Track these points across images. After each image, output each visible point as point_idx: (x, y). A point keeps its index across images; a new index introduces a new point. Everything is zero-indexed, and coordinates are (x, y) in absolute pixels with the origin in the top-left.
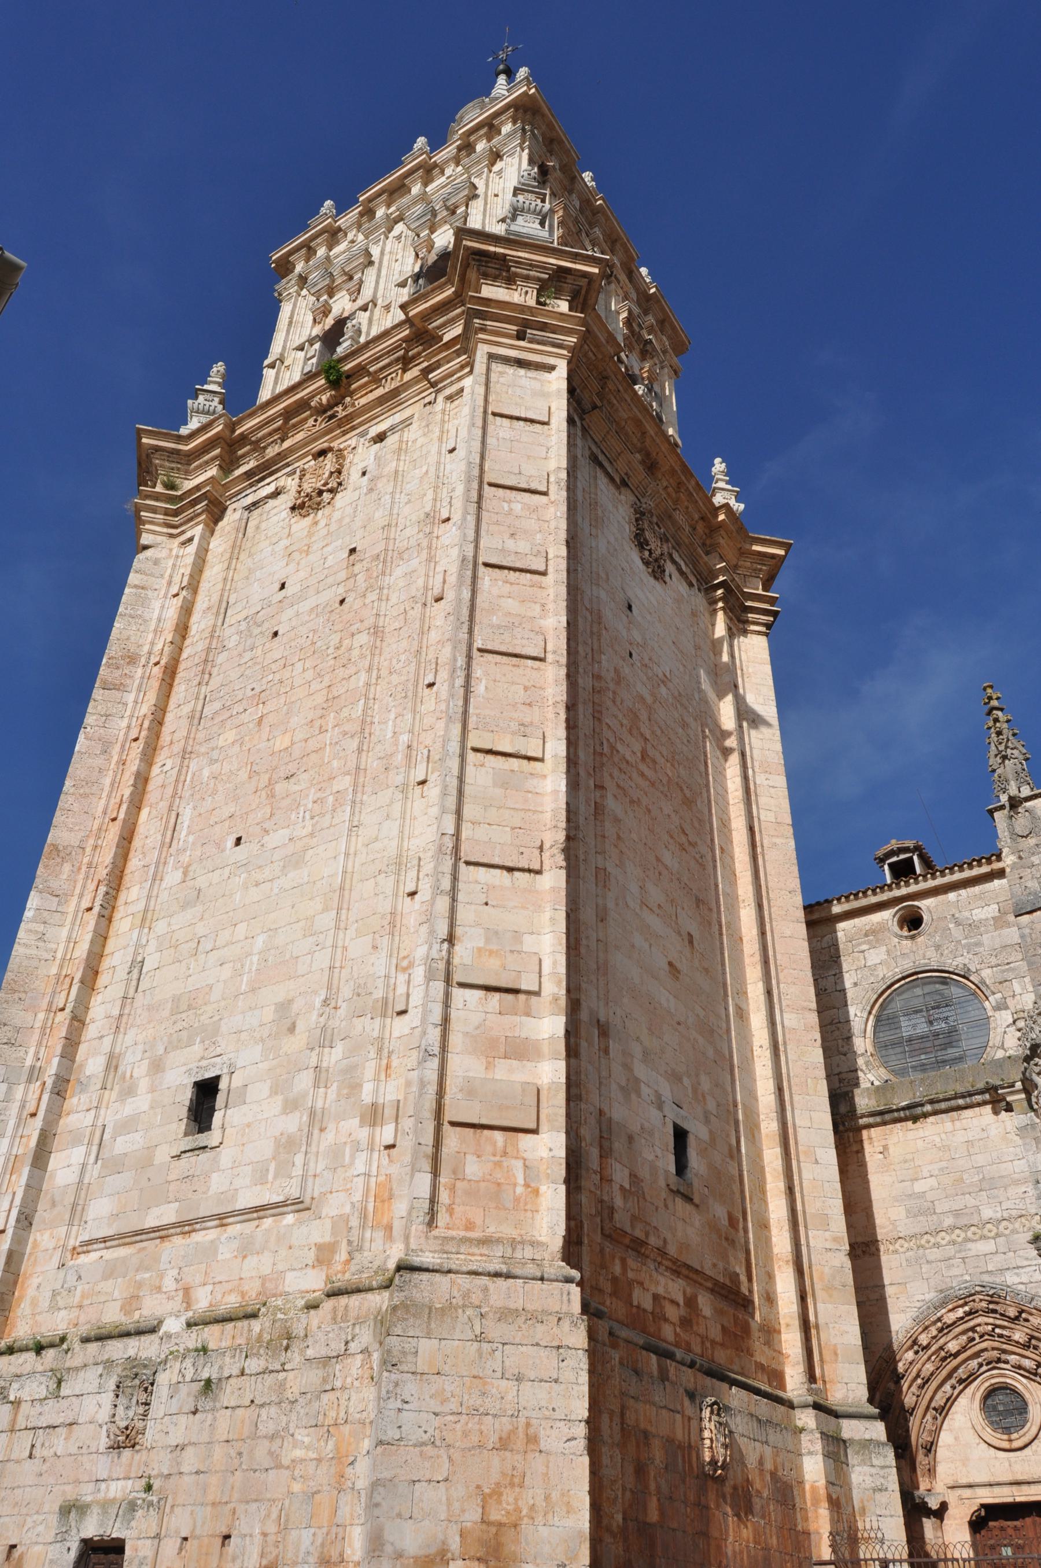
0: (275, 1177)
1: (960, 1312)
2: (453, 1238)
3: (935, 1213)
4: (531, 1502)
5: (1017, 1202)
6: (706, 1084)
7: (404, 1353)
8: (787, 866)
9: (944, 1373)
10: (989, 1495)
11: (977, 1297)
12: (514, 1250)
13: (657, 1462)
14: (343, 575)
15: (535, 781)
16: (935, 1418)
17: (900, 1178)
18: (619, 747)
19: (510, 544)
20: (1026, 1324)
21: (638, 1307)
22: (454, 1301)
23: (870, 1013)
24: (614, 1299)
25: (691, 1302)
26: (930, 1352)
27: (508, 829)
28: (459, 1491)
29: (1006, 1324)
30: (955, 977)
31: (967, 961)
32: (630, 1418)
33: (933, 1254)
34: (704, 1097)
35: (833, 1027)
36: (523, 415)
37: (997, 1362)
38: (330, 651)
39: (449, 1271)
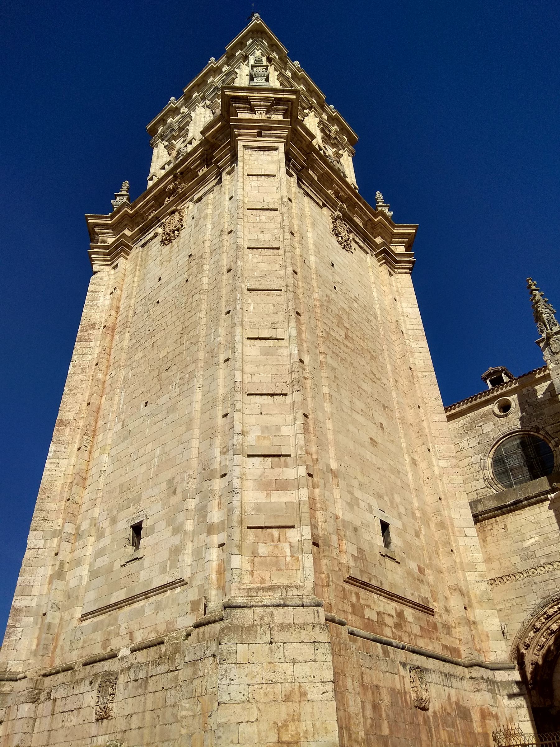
0: (170, 569)
2: (253, 588)
3: (536, 557)
4: (305, 729)
6: (397, 499)
7: (229, 653)
8: (432, 386)
12: (287, 592)
13: (386, 701)
14: (186, 268)
15: (282, 350)
17: (515, 541)
18: (332, 333)
19: (261, 236)
21: (368, 619)
22: (255, 622)
24: (353, 616)
25: (400, 615)
26: (542, 631)
27: (270, 375)
28: (264, 726)
30: (531, 433)
31: (537, 424)
32: (367, 679)
33: (537, 579)
34: (397, 506)
35: (470, 467)
36: (263, 173)
38: (183, 305)
39: (252, 606)
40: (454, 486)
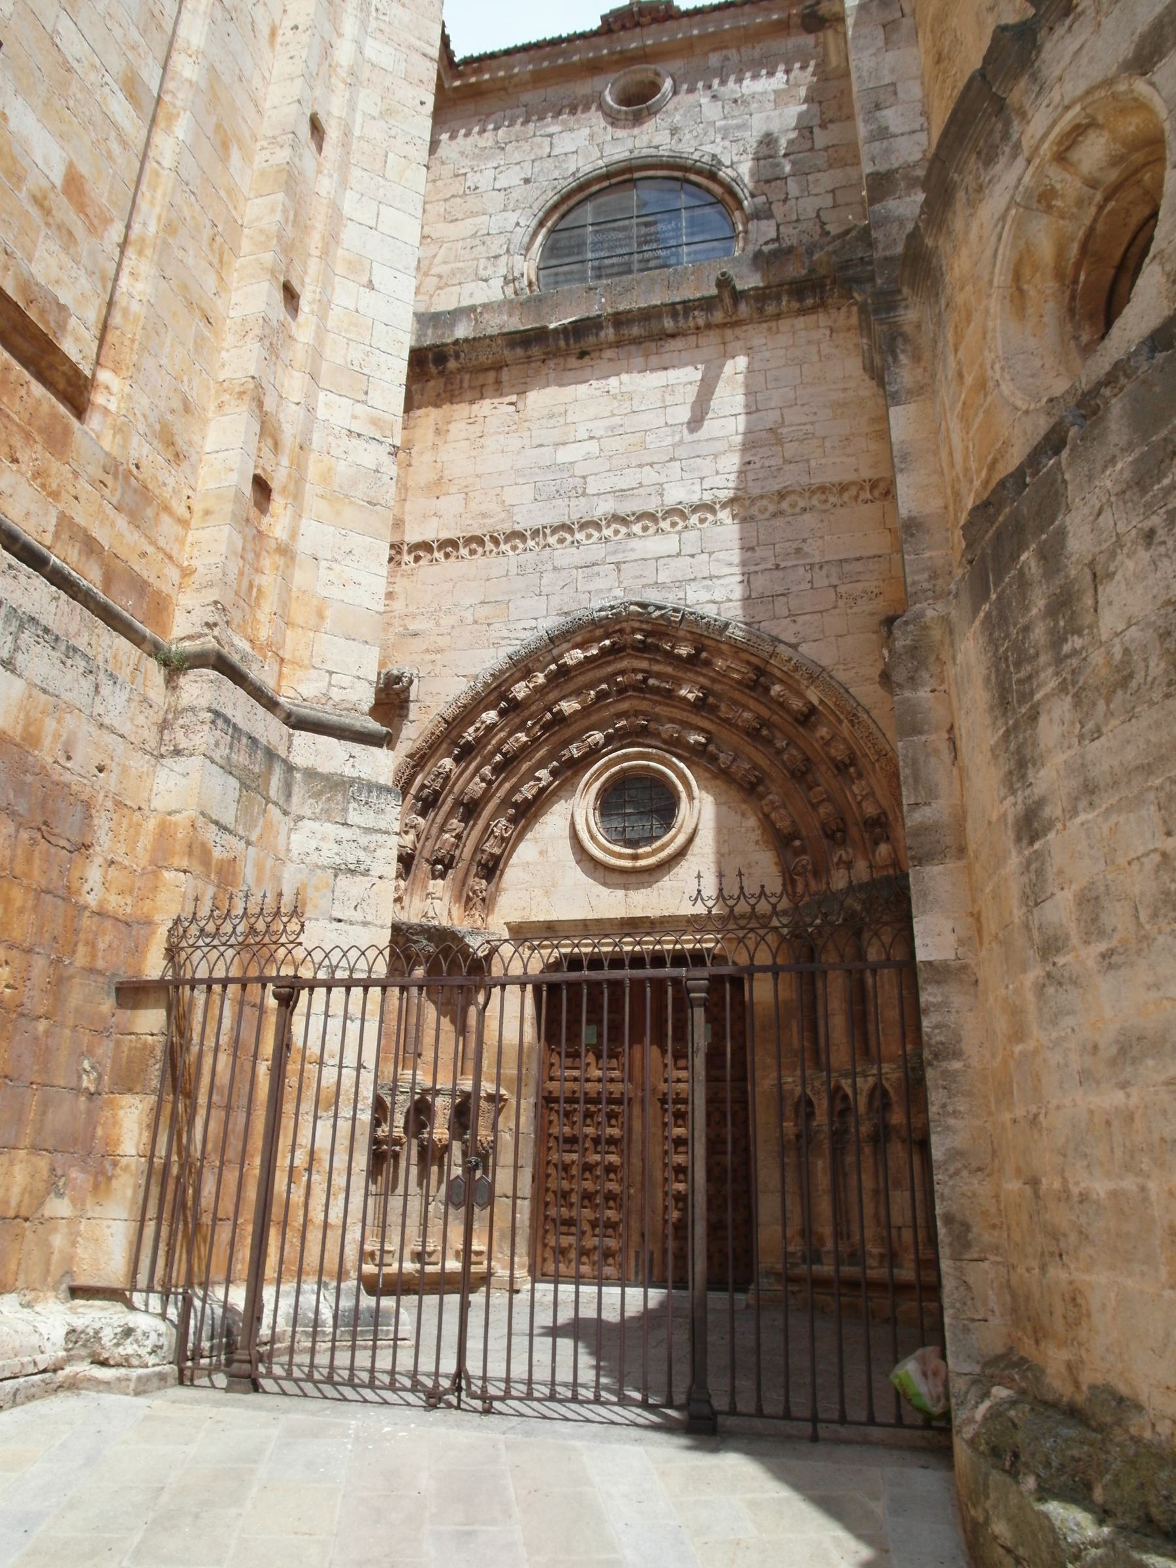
3: (584, 494)
23: (541, 224)
26: (527, 713)
29: (669, 670)
31: (717, 150)
37: (638, 735)
40: (392, 133)
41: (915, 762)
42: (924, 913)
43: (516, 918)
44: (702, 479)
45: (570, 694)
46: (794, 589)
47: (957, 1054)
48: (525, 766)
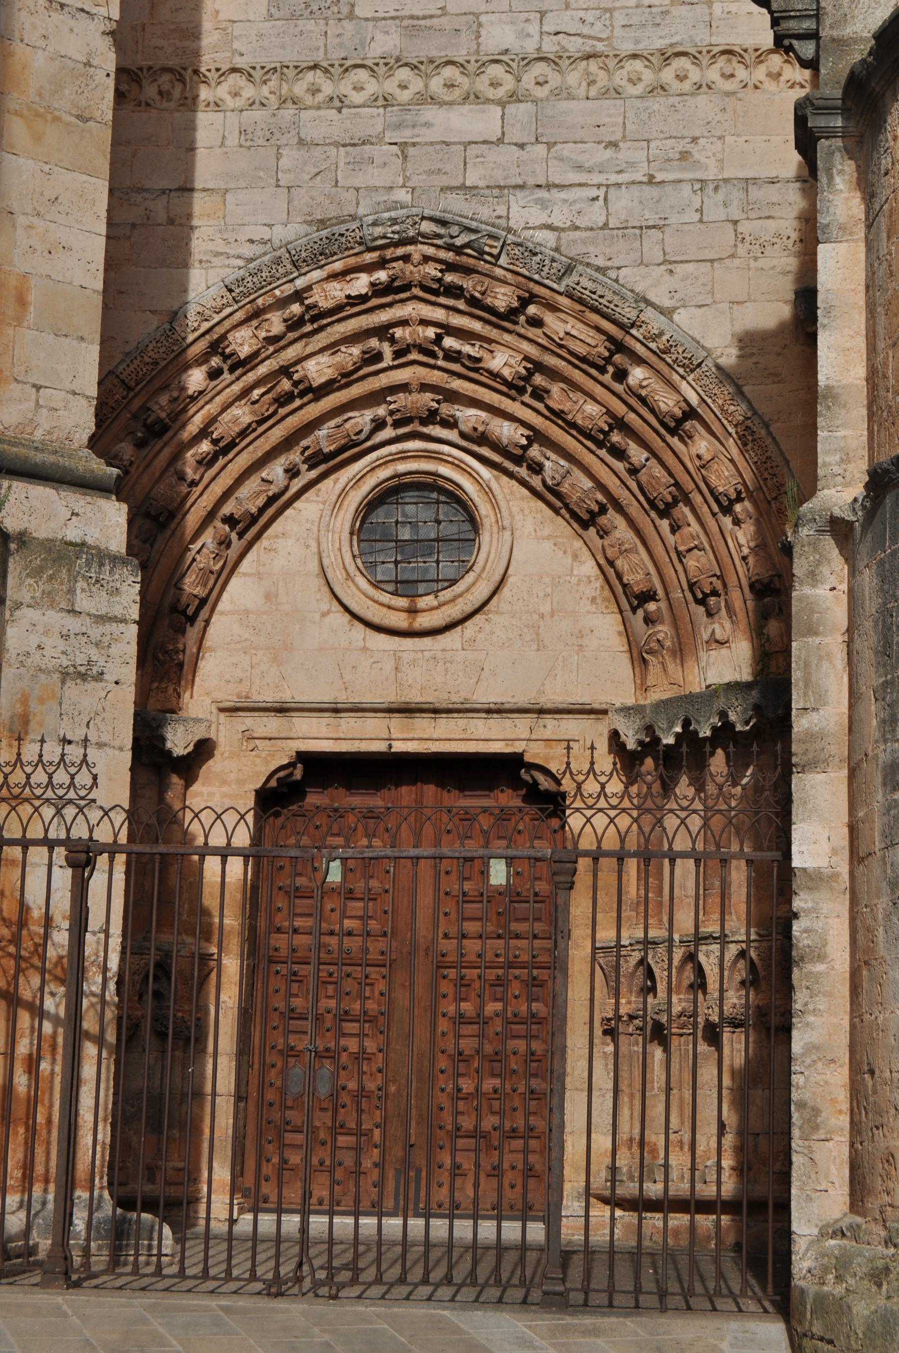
1: (361, 284)
3: (351, 16)
5: (590, 16)
9: (278, 434)
10: (324, 732)
11: (416, 251)
16: (225, 543)
20: (532, 332)
26: (251, 377)
29: (477, 326)
37: (424, 422)
41: (807, 665)
42: (803, 820)
43: (229, 698)
44: (543, 14)
45: (321, 351)
46: (672, 220)
47: (821, 958)
48: (243, 460)
